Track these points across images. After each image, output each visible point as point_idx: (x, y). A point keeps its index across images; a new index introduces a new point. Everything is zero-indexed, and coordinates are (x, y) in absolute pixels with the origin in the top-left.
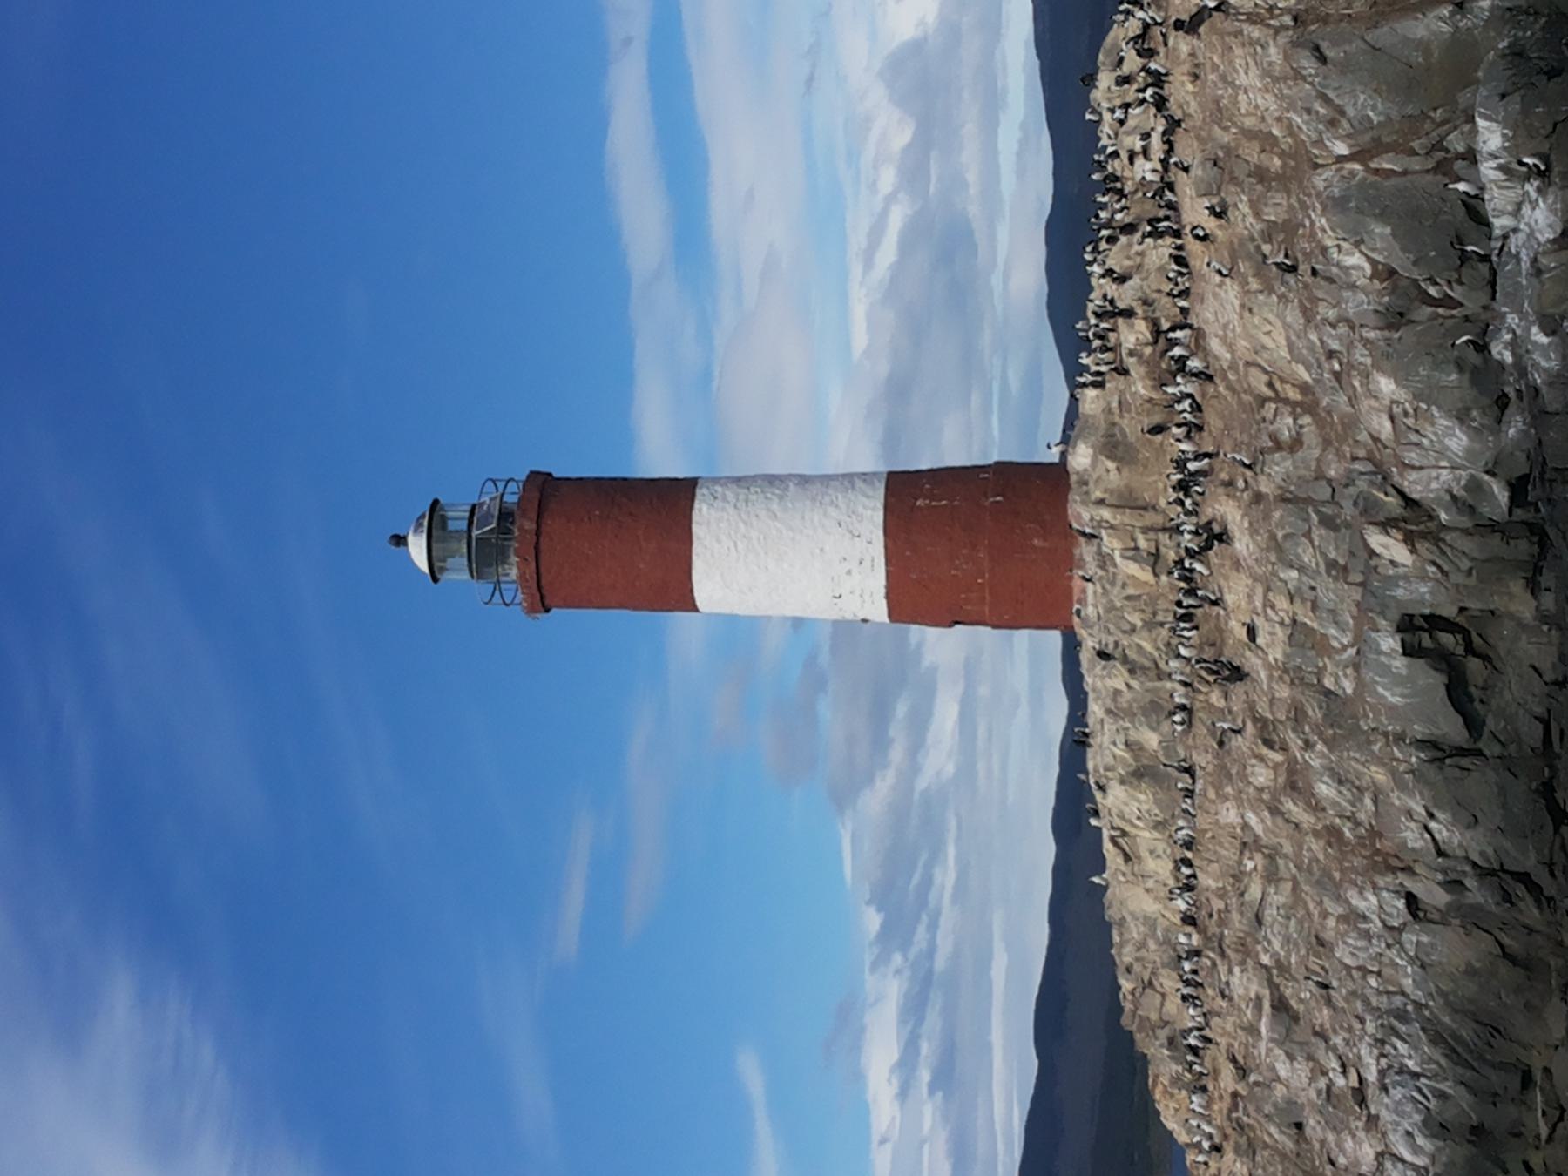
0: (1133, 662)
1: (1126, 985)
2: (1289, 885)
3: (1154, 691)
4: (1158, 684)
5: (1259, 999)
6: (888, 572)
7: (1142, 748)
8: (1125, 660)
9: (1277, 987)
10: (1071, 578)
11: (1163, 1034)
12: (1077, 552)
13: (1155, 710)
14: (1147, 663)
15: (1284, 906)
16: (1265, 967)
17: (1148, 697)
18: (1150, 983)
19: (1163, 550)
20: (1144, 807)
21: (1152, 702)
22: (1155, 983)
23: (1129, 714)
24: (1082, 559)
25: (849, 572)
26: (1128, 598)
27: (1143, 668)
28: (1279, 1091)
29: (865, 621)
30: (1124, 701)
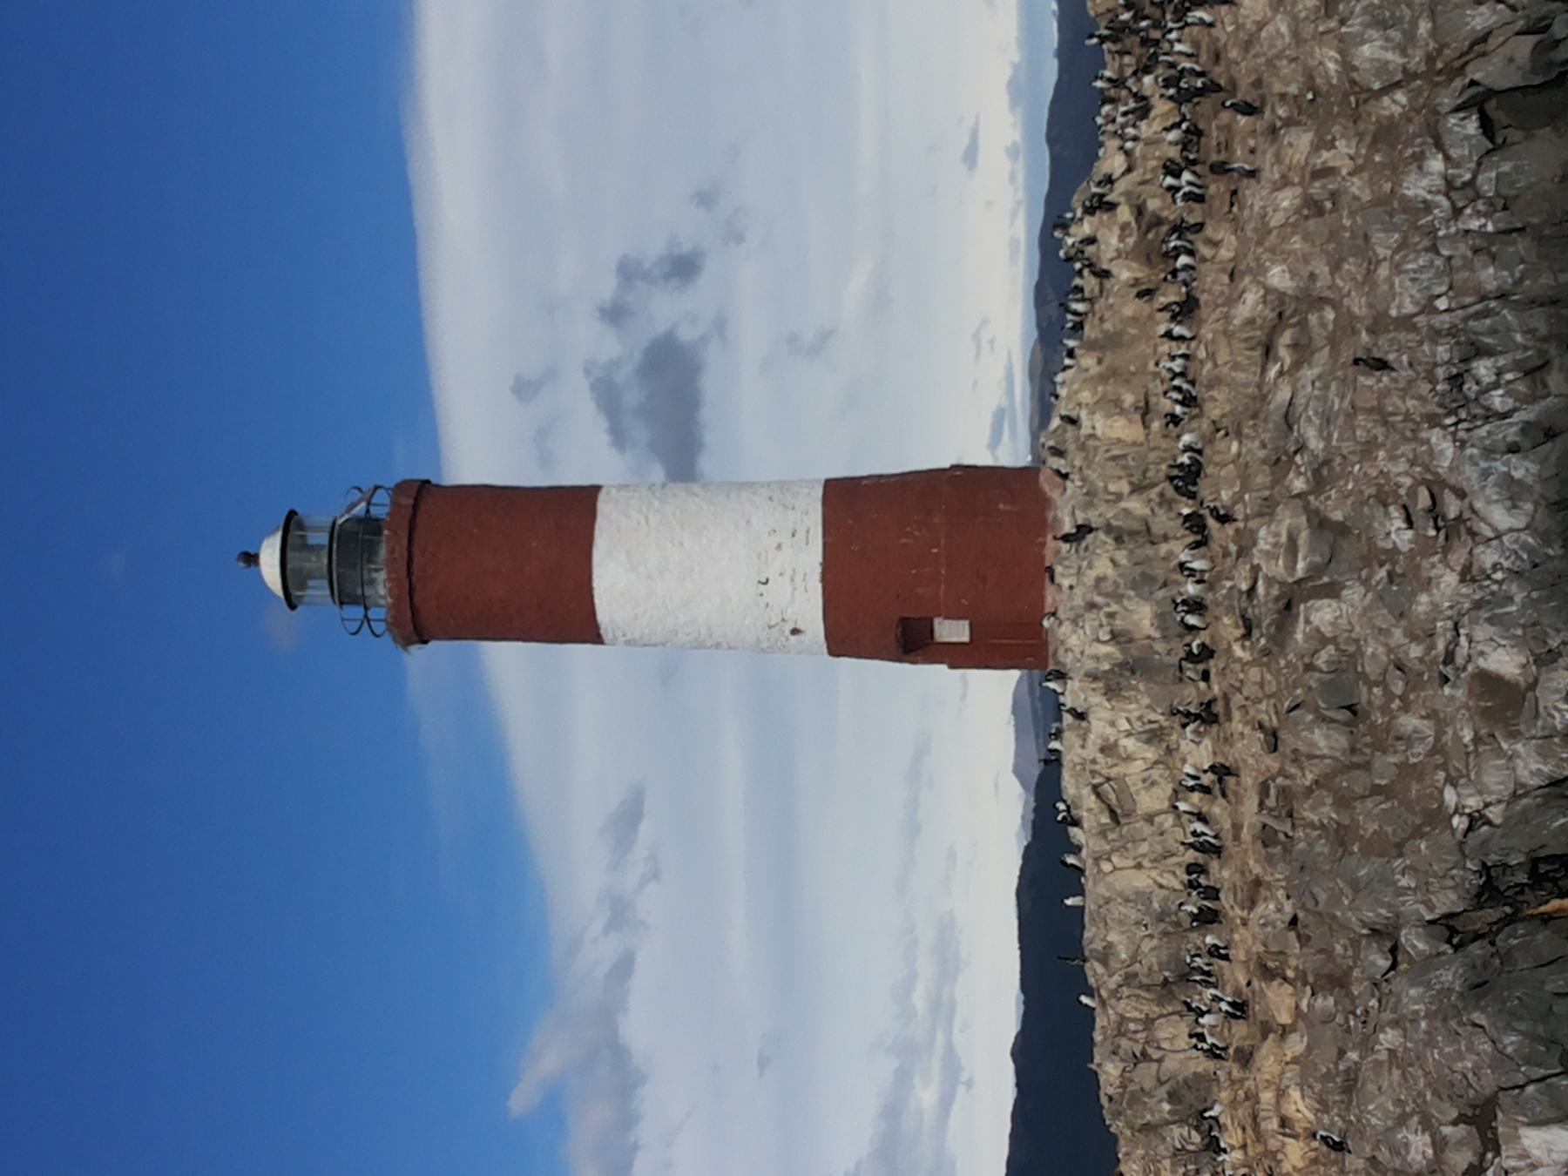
0: (1119, 528)
1: (1110, 1072)
2: (1327, 349)
3: (1148, 560)
4: (1149, 551)
5: (1292, 540)
6: (825, 544)
7: (1131, 640)
8: (1109, 529)
9: (1317, 512)
10: (1043, 544)
11: (1162, 1092)
12: (1050, 516)
13: (1143, 583)
14: (1136, 526)
15: (1319, 377)
16: (1299, 496)
17: (1138, 570)
18: (1144, 1053)
19: (1153, 400)
20: (1136, 714)
21: (1143, 574)
22: (1150, 1051)
23: (1119, 598)
24: (1056, 519)
25: (779, 547)
26: (1114, 458)
27: (1133, 534)
28: (1321, 660)
29: (795, 631)
30: (1108, 587)
